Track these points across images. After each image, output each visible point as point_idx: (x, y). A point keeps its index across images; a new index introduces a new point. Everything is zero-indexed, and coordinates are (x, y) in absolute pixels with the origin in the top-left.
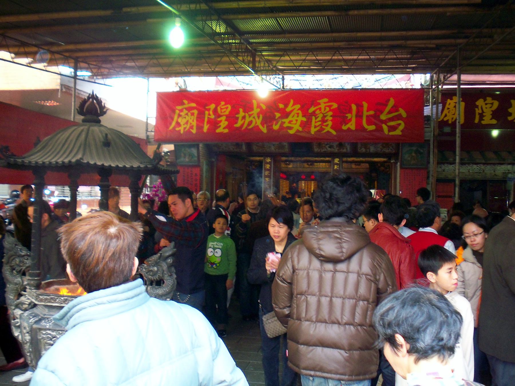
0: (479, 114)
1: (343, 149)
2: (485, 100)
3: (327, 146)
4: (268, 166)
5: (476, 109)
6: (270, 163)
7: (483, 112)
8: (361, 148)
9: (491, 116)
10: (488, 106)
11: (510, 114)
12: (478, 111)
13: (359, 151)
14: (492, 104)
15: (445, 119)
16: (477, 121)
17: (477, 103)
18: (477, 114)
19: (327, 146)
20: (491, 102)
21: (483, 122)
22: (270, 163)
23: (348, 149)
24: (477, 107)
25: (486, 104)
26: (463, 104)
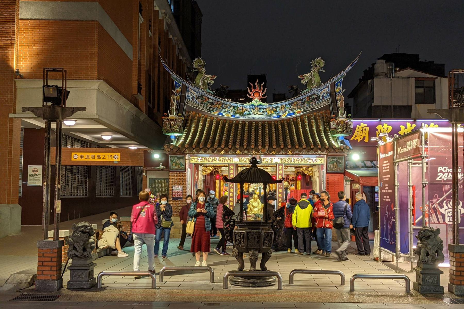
14: (388, 128)
15: (355, 139)
17: (377, 128)
20: (387, 127)
24: (377, 130)
25: (383, 128)
26: (368, 128)
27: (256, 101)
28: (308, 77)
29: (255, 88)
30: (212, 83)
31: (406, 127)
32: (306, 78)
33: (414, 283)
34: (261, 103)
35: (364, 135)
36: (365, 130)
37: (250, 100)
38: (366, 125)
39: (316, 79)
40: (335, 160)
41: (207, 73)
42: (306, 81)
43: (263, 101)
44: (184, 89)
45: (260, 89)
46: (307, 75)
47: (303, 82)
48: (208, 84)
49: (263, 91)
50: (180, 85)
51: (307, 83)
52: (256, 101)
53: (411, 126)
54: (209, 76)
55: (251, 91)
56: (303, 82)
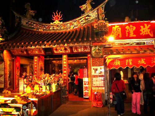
0: (127, 32)
1: (67, 51)
2: (129, 26)
3: (60, 50)
4: (36, 61)
5: (126, 31)
6: (37, 59)
7: (129, 32)
8: (75, 50)
9: (133, 33)
10: (132, 29)
11: (141, 32)
12: (127, 31)
13: (74, 52)
14: (133, 28)
16: (127, 36)
18: (127, 33)
19: (60, 50)
21: (130, 36)
22: (37, 59)
23: (69, 51)
24: (126, 29)
25: (130, 28)
26: (120, 29)
27: (57, 22)
28: (84, 6)
29: (56, 15)
30: (34, 14)
31: (144, 27)
32: (84, 7)
33: (141, 105)
34: (59, 22)
35: (118, 33)
36: (119, 29)
37: (53, 21)
38: (119, 26)
39: (89, 7)
40: (97, 48)
41: (31, 10)
42: (84, 8)
43: (60, 21)
44: (20, 19)
45: (59, 15)
46: (84, 5)
47: (82, 9)
48: (32, 15)
49: (60, 16)
50: (18, 17)
51: (84, 10)
52: (57, 22)
53: (148, 26)
54: (32, 11)
55: (54, 17)
56: (82, 9)
